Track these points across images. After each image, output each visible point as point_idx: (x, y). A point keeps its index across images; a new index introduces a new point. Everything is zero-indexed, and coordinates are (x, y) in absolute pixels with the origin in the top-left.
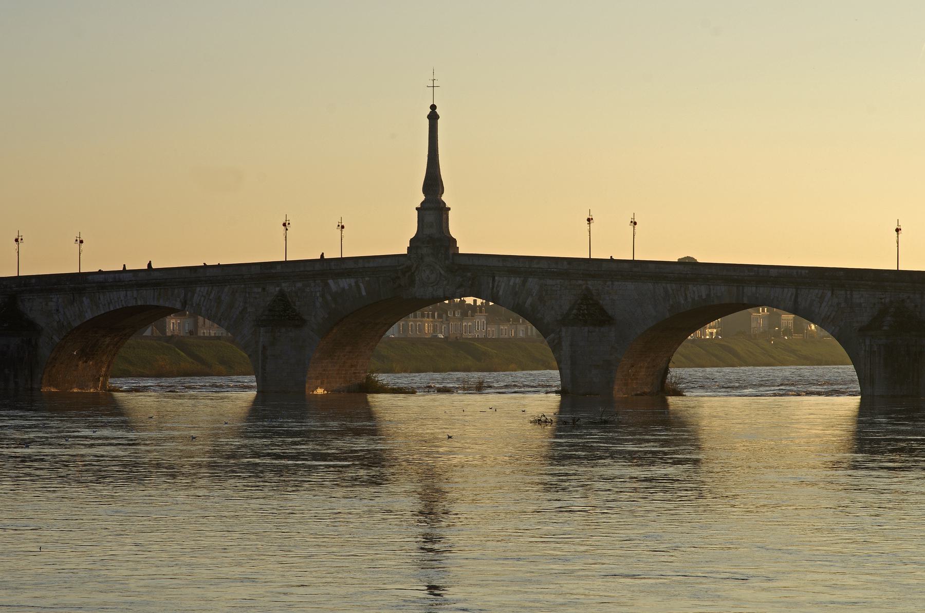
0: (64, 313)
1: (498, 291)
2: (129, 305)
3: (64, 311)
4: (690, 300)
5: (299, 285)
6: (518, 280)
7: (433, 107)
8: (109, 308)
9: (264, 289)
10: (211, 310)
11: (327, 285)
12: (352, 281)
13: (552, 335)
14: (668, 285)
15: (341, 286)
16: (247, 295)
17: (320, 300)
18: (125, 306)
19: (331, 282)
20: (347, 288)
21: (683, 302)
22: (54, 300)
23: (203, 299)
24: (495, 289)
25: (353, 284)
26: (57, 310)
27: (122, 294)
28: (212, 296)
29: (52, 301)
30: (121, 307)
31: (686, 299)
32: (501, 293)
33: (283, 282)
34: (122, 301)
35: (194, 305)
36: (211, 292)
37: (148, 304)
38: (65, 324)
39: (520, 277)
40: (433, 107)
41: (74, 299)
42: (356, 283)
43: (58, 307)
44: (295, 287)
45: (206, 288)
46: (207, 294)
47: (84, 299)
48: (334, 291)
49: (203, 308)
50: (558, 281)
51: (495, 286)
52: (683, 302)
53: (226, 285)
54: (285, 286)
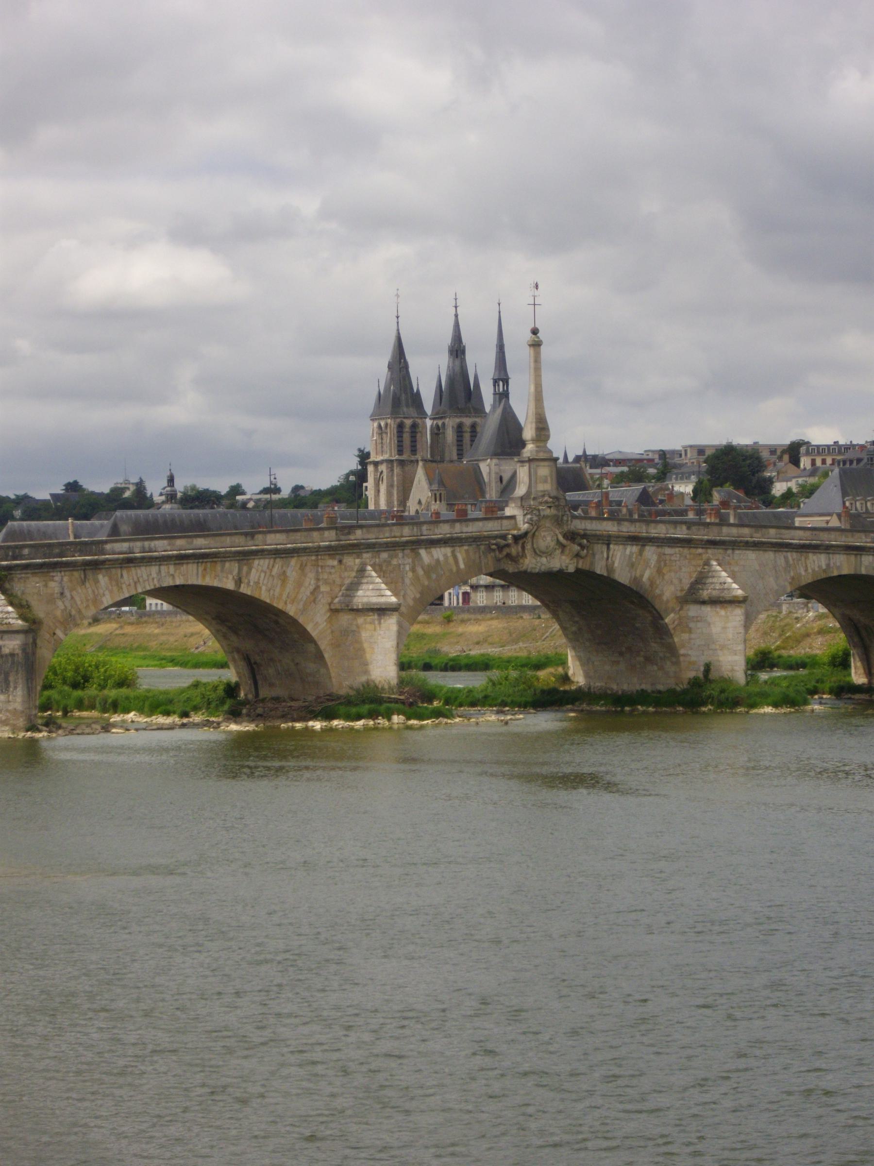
0: (72, 598)
1: (613, 563)
2: (164, 585)
3: (71, 595)
4: (810, 571)
5: (384, 555)
6: (635, 549)
7: (535, 332)
8: (136, 589)
9: (340, 562)
10: (274, 591)
11: (418, 555)
12: (448, 551)
13: (672, 615)
14: (789, 554)
15: (436, 556)
16: (320, 570)
17: (410, 574)
18: (158, 586)
19: (423, 552)
20: (441, 558)
21: (803, 573)
22: (56, 578)
23: (263, 575)
24: (610, 559)
25: (449, 554)
26: (62, 594)
27: (154, 570)
28: (275, 571)
29: (53, 580)
30: (153, 587)
31: (806, 570)
32: (616, 565)
33: (365, 553)
34: (153, 579)
35: (252, 584)
36: (273, 566)
37: (190, 583)
38: (73, 612)
39: (637, 545)
40: (535, 332)
41: (85, 577)
42: (453, 552)
43: (63, 589)
44: (379, 557)
45: (267, 561)
46: (268, 568)
47: (100, 577)
48: (426, 564)
49: (264, 588)
50: (677, 550)
51: (610, 556)
52: (803, 573)
53: (293, 557)
54: (366, 556)
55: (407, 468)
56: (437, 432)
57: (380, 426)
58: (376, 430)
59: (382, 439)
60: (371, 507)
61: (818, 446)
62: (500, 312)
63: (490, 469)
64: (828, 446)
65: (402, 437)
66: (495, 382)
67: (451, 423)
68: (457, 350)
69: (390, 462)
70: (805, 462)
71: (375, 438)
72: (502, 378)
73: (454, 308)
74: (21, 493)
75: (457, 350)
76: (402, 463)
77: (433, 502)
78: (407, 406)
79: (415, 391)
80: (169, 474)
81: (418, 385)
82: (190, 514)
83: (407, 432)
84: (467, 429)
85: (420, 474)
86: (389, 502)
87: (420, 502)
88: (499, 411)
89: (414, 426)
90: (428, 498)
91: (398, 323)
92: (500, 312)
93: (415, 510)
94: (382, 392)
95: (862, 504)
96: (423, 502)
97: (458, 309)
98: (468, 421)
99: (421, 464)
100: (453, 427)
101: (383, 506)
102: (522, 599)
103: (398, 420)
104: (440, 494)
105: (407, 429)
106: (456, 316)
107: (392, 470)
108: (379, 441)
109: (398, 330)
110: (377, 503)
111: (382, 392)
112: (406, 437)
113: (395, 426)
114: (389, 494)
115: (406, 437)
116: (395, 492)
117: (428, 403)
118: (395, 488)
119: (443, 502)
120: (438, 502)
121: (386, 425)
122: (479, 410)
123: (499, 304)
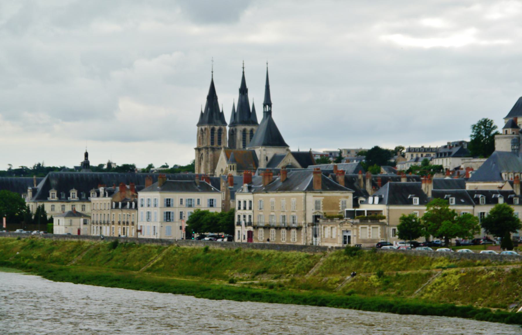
55: (216, 152)
56: (232, 134)
57: (202, 130)
58: (200, 131)
59: (203, 136)
60: (196, 173)
61: (415, 148)
62: (267, 68)
63: (261, 152)
64: (419, 149)
65: (213, 135)
66: (265, 105)
67: (240, 128)
68: (243, 91)
69: (207, 148)
70: (408, 156)
71: (199, 136)
72: (268, 102)
73: (242, 69)
74: (62, 166)
75: (243, 91)
76: (213, 149)
77: (230, 170)
78: (217, 119)
79: (221, 111)
80: (85, 151)
81: (222, 108)
82: (93, 174)
83: (216, 133)
84: (248, 132)
85: (222, 155)
86: (206, 170)
87: (222, 170)
88: (266, 122)
89: (220, 130)
90: (227, 168)
91: (212, 75)
92: (267, 68)
93: (219, 174)
94: (203, 112)
95: (506, 175)
96: (224, 170)
97: (244, 69)
98: (248, 128)
99: (223, 149)
100: (241, 131)
101: (202, 172)
102: (290, 238)
103: (212, 126)
104: (233, 166)
105: (216, 131)
106: (243, 72)
107: (208, 153)
108: (201, 138)
109: (212, 79)
110: (199, 171)
111: (203, 112)
112: (216, 135)
113: (210, 130)
114: (206, 166)
115: (216, 135)
116: (209, 165)
117: (228, 118)
118: (209, 163)
119: (235, 170)
120: (232, 170)
121: (205, 129)
122: (255, 123)
123: (267, 64)
